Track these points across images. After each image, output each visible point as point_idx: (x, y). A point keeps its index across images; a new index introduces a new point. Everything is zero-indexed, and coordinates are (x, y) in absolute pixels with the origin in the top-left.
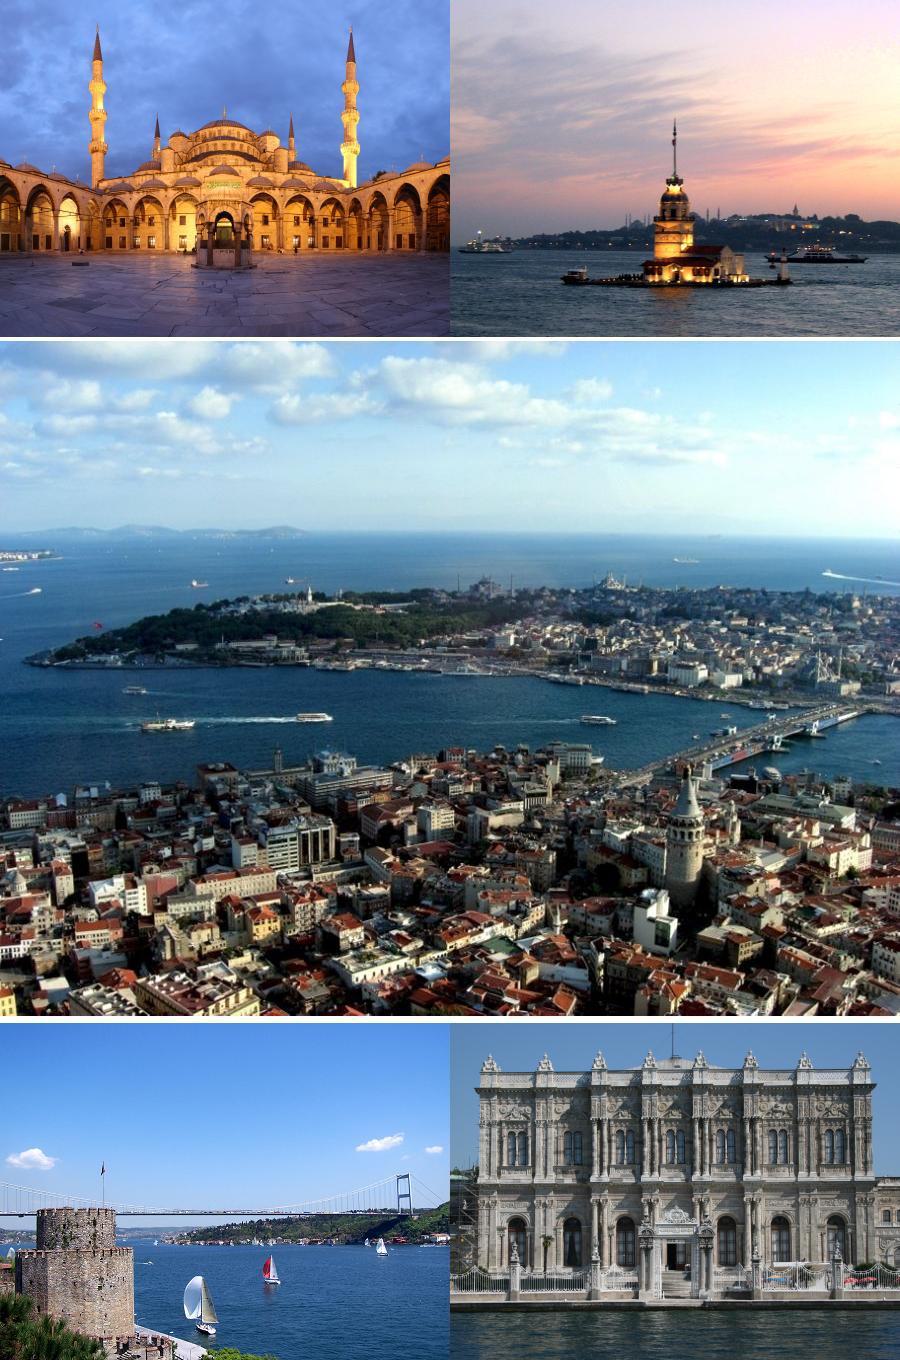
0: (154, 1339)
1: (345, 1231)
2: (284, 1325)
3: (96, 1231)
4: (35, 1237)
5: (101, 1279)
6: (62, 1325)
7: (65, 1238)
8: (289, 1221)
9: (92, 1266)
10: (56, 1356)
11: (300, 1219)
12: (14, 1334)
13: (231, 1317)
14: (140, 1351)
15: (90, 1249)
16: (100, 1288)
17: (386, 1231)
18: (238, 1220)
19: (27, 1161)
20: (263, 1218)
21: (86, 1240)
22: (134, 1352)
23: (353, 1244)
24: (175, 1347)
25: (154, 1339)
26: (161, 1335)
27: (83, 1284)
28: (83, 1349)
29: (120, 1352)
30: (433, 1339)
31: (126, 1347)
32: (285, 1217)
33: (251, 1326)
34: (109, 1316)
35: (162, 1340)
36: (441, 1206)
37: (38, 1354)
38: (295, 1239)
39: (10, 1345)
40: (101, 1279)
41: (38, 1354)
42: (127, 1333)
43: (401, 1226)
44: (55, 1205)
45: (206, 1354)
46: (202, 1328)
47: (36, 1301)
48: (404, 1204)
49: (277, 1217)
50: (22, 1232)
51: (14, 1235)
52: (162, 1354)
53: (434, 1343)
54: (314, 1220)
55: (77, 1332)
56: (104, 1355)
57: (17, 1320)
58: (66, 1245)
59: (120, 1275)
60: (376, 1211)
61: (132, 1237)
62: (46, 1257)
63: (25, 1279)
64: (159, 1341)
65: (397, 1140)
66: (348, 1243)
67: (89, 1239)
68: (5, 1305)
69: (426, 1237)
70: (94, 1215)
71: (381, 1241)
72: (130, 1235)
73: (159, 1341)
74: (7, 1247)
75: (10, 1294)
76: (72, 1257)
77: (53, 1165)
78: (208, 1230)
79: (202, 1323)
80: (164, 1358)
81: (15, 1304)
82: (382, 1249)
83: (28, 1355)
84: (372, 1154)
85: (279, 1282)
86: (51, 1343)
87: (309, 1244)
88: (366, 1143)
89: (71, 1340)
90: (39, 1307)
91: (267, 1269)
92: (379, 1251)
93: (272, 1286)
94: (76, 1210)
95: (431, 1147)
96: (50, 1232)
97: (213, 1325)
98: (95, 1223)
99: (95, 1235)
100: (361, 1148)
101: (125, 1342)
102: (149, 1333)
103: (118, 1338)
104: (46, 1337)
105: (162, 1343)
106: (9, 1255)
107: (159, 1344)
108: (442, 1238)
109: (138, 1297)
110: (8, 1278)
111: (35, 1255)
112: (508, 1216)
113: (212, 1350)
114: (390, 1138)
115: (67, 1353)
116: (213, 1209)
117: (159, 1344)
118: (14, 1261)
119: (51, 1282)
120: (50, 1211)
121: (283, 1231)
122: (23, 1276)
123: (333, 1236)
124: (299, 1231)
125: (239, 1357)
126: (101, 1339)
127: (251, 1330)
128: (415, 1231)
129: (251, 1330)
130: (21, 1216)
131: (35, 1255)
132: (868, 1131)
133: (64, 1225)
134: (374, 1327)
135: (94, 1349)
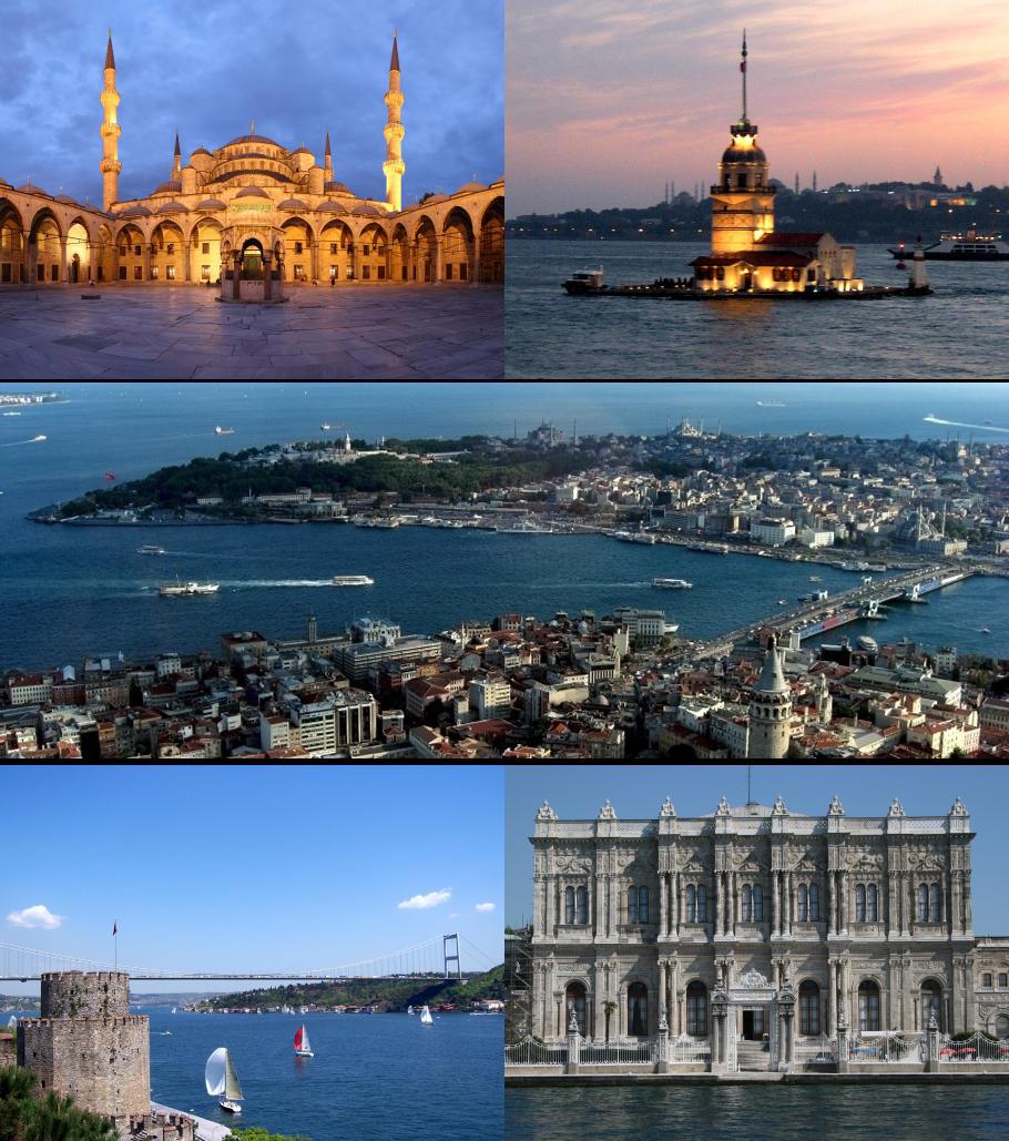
0: (173, 1118)
1: (386, 998)
2: (318, 1102)
3: (107, 998)
4: (39, 1004)
5: (113, 1051)
6: (69, 1102)
7: (72, 1006)
8: (322, 987)
10: (63, 1137)
11: (336, 984)
12: (15, 1112)
13: (258, 1093)
14: (157, 1131)
15: (101, 1017)
16: (112, 1060)
17: (432, 997)
18: (266, 985)
19: (31, 919)
20: (294, 983)
21: (96, 1007)
22: (151, 1132)
23: (394, 1011)
24: (197, 1126)
25: (173, 1118)
26: (180, 1113)
27: (93, 1057)
28: (93, 1129)
29: (135, 1132)
30: (485, 1118)
31: (141, 1126)
32: (319, 982)
33: (280, 1104)
34: (122, 1092)
35: (181, 1119)
36: (493, 970)
37: (42, 1134)
38: (330, 1006)
39: (11, 1124)
40: (113, 1051)
41: (42, 1134)
42: (142, 1111)
43: (448, 992)
44: (61, 968)
45: (230, 1134)
46: (226, 1105)
47: (40, 1074)
48: (452, 967)
49: (309, 982)
50: (25, 998)
51: (15, 1002)
52: (181, 1134)
53: (485, 1122)
54: (351, 985)
55: (86, 1111)
56: (116, 1135)
57: (19, 1097)
58: (73, 1013)
59: (134, 1047)
60: (420, 975)
61: (148, 1004)
63: (28, 1051)
64: (178, 1121)
65: (444, 896)
66: (389, 1011)
68: (6, 1080)
69: (477, 1004)
71: (426, 1008)
72: (145, 1001)
73: (178, 1121)
74: (8, 1015)
75: (11, 1068)
77: (59, 924)
78: (232, 996)
79: (226, 1100)
80: (183, 1140)
81: (17, 1079)
82: (427, 1018)
83: (32, 1135)
84: (416, 911)
85: (312, 1055)
86: (57, 1122)
87: (346, 1011)
88: (409, 900)
89: (79, 1119)
90: (43, 1083)
91: (298, 1040)
92: (423, 1020)
93: (305, 1059)
94: (85, 974)
95: (482, 903)
96: (55, 998)
97: (238, 1102)
98: (106, 989)
99: (106, 1002)
100: (404, 905)
101: (140, 1121)
102: (167, 1111)
103: (131, 1117)
104: (52, 1116)
105: (181, 1123)
106: (10, 1024)
107: (178, 1123)
108: (494, 1005)
109: (154, 1070)
110: (10, 1050)
111: (39, 1024)
112: (567, 980)
113: (236, 1130)
114: (435, 894)
115: (74, 1134)
116: (239, 973)
117: (178, 1123)
118: (15, 1029)
119: (57, 1054)
120: (56, 975)
121: (317, 997)
122: (27, 1049)
123: (372, 1003)
124: (335, 998)
125: (267, 1137)
126: (113, 1118)
127: (281, 1108)
128: (464, 997)
129: (281, 1108)
130: (24, 980)
131: (39, 1024)
132: (967, 885)
134: (419, 1104)
135: (105, 1129)
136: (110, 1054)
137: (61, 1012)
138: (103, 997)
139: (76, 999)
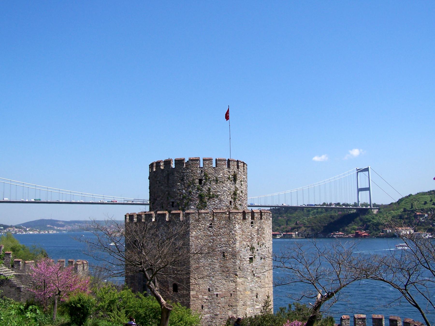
3: (236, 189)
5: (252, 248)
7: (201, 197)
9: (243, 231)
40: (252, 248)
58: (203, 205)
67: (230, 199)
76: (220, 220)
98: (235, 179)
99: (235, 194)
120: (179, 162)
133: (200, 181)
136: (250, 253)
138: (233, 189)
139: (205, 189)
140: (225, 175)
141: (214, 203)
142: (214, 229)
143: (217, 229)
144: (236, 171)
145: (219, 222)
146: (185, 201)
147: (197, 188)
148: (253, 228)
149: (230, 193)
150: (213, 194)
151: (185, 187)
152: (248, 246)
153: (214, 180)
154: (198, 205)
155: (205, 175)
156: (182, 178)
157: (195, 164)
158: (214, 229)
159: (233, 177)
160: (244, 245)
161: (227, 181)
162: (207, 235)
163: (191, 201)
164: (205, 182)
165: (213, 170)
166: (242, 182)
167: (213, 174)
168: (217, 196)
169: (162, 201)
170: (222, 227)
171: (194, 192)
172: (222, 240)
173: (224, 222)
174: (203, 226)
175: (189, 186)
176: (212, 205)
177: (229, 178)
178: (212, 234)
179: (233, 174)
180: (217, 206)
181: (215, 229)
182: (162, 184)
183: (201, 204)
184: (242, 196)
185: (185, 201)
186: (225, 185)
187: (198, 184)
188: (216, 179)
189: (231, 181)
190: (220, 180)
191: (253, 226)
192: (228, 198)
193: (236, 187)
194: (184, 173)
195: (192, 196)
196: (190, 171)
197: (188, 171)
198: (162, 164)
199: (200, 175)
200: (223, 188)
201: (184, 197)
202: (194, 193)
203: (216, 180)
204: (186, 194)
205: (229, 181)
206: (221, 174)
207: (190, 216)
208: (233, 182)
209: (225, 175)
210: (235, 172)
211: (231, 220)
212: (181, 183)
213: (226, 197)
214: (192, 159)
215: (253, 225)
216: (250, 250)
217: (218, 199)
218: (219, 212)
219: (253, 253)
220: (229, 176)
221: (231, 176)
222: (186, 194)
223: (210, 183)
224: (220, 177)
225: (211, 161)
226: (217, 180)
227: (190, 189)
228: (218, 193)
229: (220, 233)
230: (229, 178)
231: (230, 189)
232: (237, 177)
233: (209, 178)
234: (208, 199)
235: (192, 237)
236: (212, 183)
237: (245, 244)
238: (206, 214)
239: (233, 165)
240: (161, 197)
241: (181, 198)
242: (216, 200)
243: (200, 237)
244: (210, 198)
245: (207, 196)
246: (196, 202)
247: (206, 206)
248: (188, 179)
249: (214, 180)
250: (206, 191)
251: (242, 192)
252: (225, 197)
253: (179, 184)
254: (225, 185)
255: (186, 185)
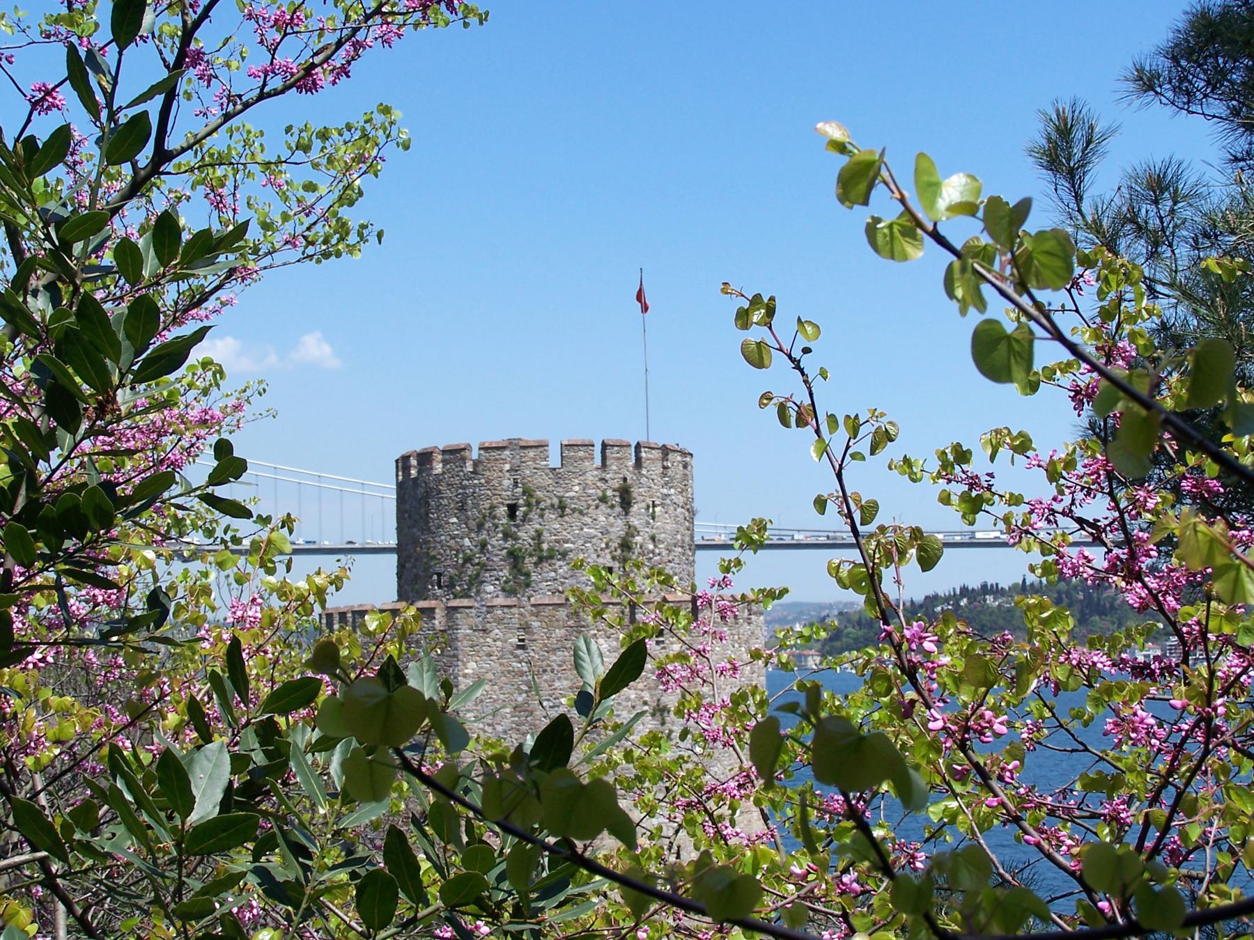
3: (631, 531)
7: (515, 558)
58: (519, 583)
62: (452, 626)
70: (623, 467)
76: (550, 624)
98: (626, 498)
99: (626, 545)
120: (455, 454)
133: (512, 509)
137: (476, 581)
138: (618, 529)
139: (525, 535)
140: (590, 491)
141: (553, 574)
142: (532, 654)
143: (542, 653)
144: (629, 476)
145: (546, 633)
146: (471, 570)
147: (503, 532)
148: (663, 648)
149: (607, 544)
150: (551, 550)
151: (471, 530)
152: (645, 703)
153: (552, 506)
154: (506, 582)
155: (524, 493)
156: (461, 502)
157: (497, 460)
158: (532, 654)
159: (617, 494)
160: (628, 699)
161: (597, 507)
162: (509, 672)
163: (487, 570)
164: (526, 514)
165: (551, 476)
166: (657, 509)
167: (551, 488)
168: (564, 555)
169: (415, 571)
170: (555, 646)
171: (495, 543)
172: (557, 684)
173: (563, 631)
174: (499, 643)
175: (480, 526)
176: (547, 581)
177: (603, 499)
178: (525, 669)
179: (617, 486)
180: (562, 583)
181: (534, 653)
182: (415, 521)
183: (514, 578)
184: (657, 551)
185: (471, 570)
186: (589, 520)
187: (504, 521)
188: (560, 502)
189: (612, 507)
190: (573, 506)
191: (663, 642)
192: (601, 560)
193: (630, 527)
194: (464, 487)
195: (488, 555)
196: (483, 481)
197: (476, 482)
198: (414, 462)
199: (509, 493)
200: (582, 529)
201: (468, 560)
202: (493, 546)
203: (559, 507)
204: (471, 550)
205: (603, 507)
206: (577, 488)
207: (459, 615)
208: (618, 509)
209: (590, 491)
210: (625, 479)
211: (583, 626)
212: (458, 518)
213: (594, 556)
214: (487, 445)
215: (661, 639)
216: (653, 715)
217: (568, 564)
218: (547, 602)
219: (663, 723)
220: (604, 491)
221: (609, 493)
222: (471, 550)
223: (542, 516)
224: (572, 498)
225: (541, 449)
226: (562, 507)
227: (484, 536)
228: (566, 545)
229: (549, 665)
230: (603, 499)
231: (608, 532)
232: (634, 495)
233: (538, 503)
234: (536, 564)
235: (465, 676)
236: (546, 516)
237: (633, 697)
238: (506, 610)
239: (619, 459)
240: (412, 560)
241: (460, 561)
242: (561, 567)
243: (490, 676)
244: (541, 560)
245: (531, 555)
246: (501, 573)
247: (528, 585)
248: (476, 506)
249: (552, 506)
250: (530, 541)
251: (653, 538)
252: (589, 557)
253: (455, 520)
254: (589, 520)
255: (473, 524)
